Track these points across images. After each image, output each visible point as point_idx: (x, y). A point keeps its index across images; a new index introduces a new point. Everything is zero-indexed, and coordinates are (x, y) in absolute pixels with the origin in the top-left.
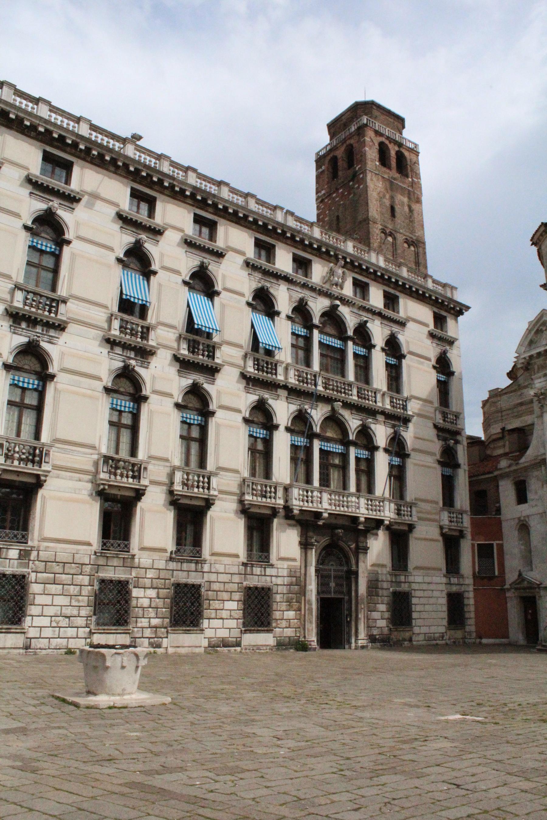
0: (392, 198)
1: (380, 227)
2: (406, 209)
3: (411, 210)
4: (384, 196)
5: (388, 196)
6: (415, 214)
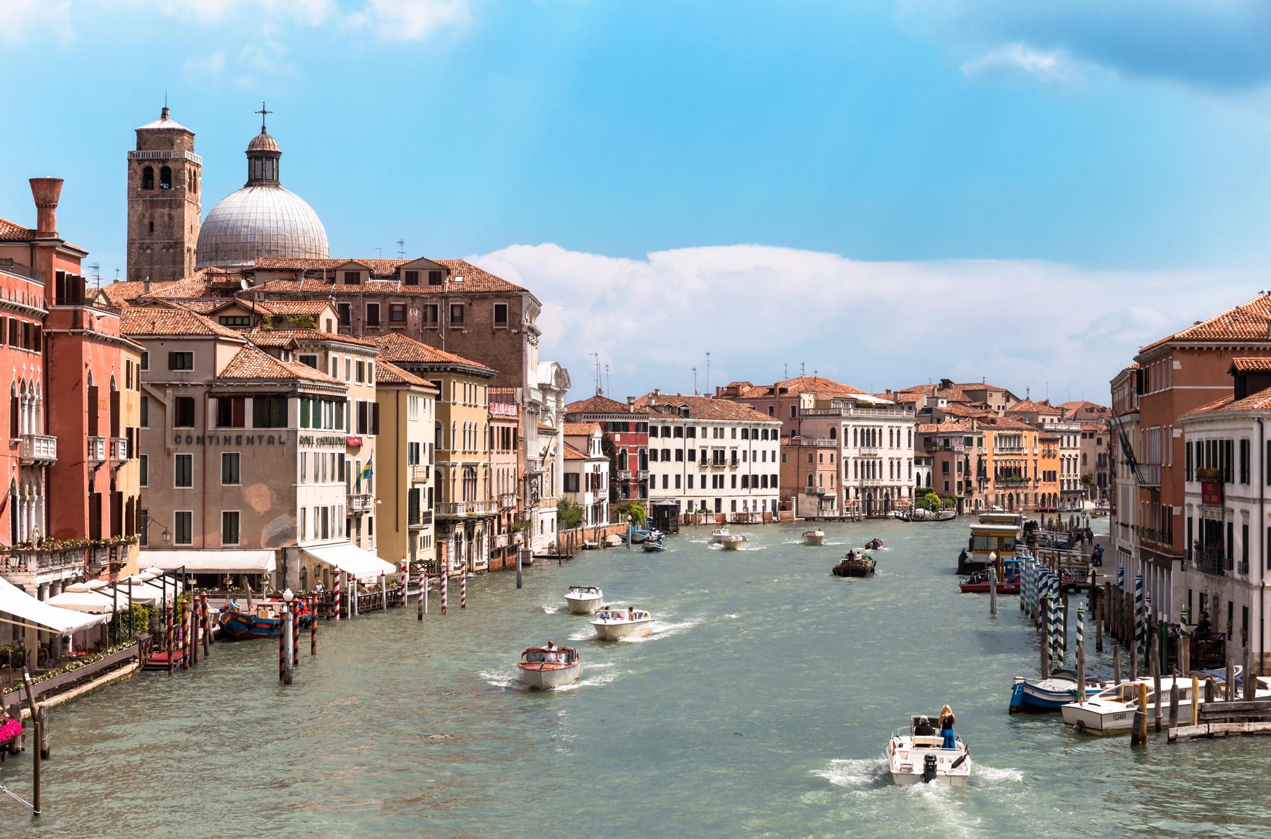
0: (152, 215)
1: (138, 245)
2: (166, 219)
3: (171, 217)
4: (144, 216)
5: (147, 215)
6: (176, 220)
